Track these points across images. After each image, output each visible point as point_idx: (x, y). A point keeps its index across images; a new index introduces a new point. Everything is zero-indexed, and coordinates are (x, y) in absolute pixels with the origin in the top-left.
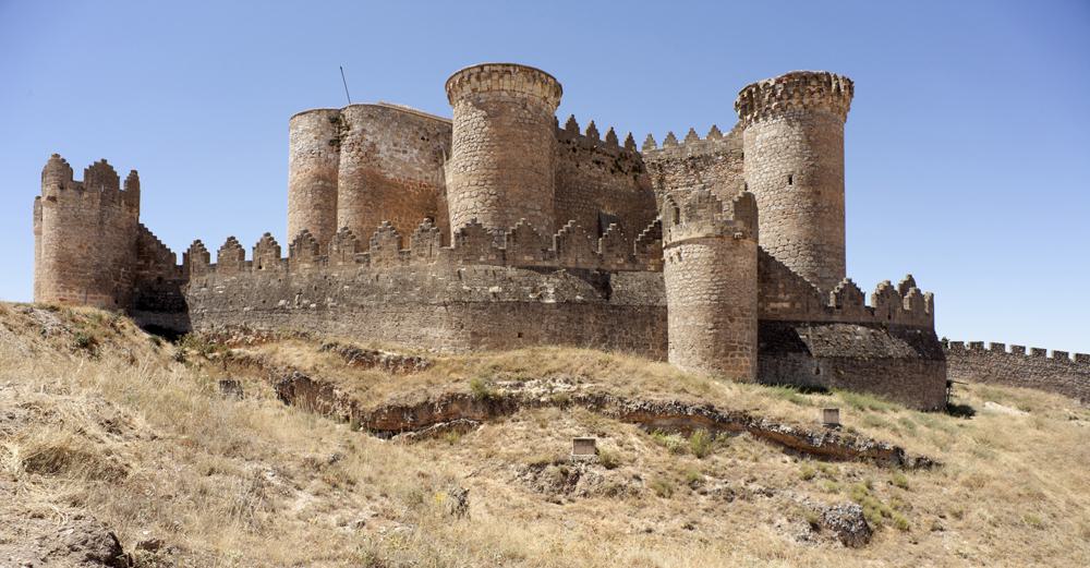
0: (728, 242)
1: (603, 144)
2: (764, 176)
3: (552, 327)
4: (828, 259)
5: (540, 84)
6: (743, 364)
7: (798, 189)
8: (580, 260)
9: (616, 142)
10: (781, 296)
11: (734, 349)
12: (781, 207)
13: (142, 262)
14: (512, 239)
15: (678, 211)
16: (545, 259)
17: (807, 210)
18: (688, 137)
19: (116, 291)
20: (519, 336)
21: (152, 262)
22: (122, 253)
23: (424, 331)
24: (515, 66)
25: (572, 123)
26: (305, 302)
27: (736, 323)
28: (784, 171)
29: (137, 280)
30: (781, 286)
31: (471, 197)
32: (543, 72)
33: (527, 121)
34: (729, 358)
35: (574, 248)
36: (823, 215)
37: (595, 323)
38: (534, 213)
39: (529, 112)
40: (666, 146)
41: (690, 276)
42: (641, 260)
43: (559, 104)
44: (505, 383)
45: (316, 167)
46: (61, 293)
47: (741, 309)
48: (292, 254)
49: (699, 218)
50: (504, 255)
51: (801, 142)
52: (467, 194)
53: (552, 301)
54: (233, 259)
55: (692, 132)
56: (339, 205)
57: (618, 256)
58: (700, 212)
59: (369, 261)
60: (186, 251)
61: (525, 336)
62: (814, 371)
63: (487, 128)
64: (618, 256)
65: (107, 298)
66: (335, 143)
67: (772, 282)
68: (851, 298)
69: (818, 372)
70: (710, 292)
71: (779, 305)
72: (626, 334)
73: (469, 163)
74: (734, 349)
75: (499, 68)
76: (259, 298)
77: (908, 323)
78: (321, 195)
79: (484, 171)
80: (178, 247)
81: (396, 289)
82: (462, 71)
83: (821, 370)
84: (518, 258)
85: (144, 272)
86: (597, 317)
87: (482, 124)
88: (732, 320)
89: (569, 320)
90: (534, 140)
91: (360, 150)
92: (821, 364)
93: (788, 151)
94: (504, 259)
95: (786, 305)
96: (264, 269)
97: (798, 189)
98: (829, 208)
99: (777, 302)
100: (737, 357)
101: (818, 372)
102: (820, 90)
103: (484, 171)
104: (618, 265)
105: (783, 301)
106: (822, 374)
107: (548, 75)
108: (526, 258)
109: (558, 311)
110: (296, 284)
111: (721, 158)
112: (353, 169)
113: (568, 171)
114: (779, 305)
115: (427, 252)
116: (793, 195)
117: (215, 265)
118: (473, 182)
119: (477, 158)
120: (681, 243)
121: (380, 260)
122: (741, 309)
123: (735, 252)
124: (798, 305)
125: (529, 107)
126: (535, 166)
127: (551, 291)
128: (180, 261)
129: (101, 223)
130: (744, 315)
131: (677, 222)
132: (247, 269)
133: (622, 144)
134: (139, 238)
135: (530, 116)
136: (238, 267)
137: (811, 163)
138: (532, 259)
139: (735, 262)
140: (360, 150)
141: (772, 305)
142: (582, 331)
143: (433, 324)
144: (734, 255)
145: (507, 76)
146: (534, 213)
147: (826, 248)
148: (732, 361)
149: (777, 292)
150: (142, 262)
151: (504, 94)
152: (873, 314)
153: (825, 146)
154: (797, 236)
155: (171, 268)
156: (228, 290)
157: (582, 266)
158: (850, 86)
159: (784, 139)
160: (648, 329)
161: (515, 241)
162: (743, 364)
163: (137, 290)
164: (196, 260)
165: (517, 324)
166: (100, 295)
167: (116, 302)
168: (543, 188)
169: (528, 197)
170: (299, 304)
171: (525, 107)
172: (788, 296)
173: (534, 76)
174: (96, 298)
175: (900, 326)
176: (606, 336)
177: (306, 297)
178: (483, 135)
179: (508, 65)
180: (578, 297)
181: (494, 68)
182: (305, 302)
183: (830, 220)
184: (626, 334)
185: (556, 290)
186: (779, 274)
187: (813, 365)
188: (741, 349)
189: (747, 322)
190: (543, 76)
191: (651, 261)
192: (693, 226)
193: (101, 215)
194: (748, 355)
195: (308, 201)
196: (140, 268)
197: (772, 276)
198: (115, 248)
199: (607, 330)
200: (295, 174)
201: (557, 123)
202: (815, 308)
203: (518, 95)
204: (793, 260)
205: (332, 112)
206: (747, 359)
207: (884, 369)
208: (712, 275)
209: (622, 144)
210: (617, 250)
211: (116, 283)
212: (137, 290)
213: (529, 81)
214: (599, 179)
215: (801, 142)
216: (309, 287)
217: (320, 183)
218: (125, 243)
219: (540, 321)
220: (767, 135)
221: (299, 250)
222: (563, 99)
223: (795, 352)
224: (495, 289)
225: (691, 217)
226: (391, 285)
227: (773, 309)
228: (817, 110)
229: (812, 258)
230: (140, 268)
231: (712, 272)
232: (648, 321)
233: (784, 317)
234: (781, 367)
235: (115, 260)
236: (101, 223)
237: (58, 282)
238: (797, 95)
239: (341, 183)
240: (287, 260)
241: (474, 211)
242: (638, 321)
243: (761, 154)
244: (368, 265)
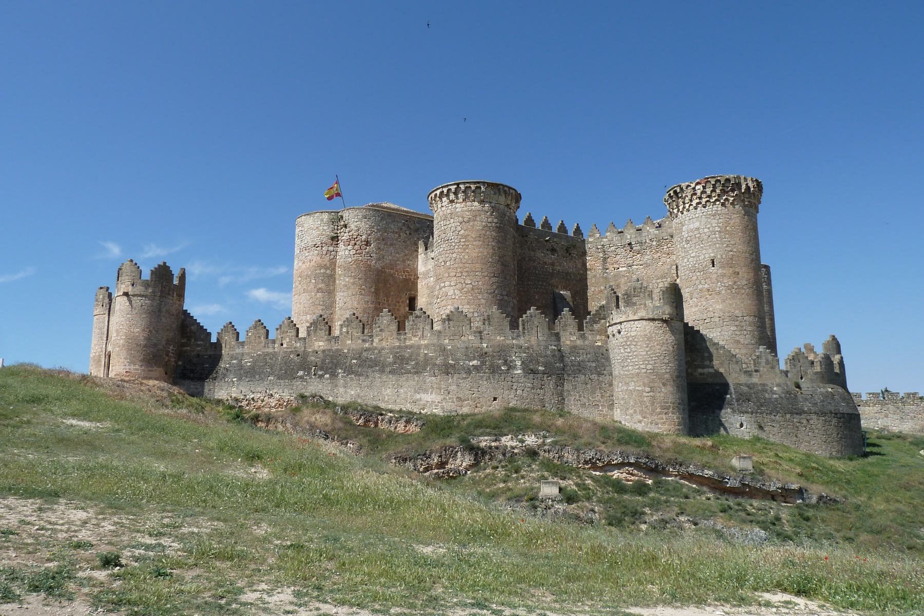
1: (555, 235)
2: (691, 259)
5: (503, 195)
7: (720, 271)
9: (566, 232)
12: (706, 286)
13: (184, 341)
14: (487, 323)
15: (617, 298)
16: (513, 339)
17: (730, 288)
19: (166, 365)
21: (193, 340)
22: (172, 334)
23: (418, 396)
25: (530, 220)
26: (320, 373)
28: (707, 256)
29: (180, 355)
31: (450, 286)
32: (506, 186)
41: (629, 350)
42: (590, 337)
43: (519, 207)
44: (486, 438)
45: (319, 258)
46: (128, 367)
48: (309, 334)
49: (635, 304)
51: (720, 232)
52: (447, 283)
53: (519, 372)
54: (259, 337)
56: (338, 288)
58: (635, 299)
59: (372, 341)
60: (220, 331)
63: (462, 231)
65: (159, 371)
70: (646, 362)
71: (706, 370)
73: (448, 259)
76: (281, 370)
78: (323, 280)
79: (461, 265)
80: (214, 329)
81: (395, 363)
82: (442, 187)
85: (186, 348)
87: (459, 228)
91: (355, 244)
93: (710, 239)
94: (481, 338)
96: (285, 346)
97: (720, 271)
99: (703, 368)
103: (461, 265)
104: (571, 341)
110: (313, 358)
111: (654, 243)
112: (350, 260)
113: (527, 259)
115: (420, 333)
117: (244, 342)
118: (453, 274)
119: (454, 255)
120: (621, 323)
121: (382, 340)
127: (519, 363)
128: (214, 339)
129: (160, 311)
131: (618, 306)
132: (270, 345)
133: (571, 233)
134: (183, 321)
136: (263, 344)
137: (729, 249)
140: (355, 244)
141: (700, 370)
143: (425, 391)
150: (184, 341)
154: (721, 310)
155: (208, 345)
156: (255, 362)
158: (759, 185)
159: (706, 230)
160: (598, 393)
161: (489, 324)
163: (180, 363)
164: (228, 338)
166: (155, 368)
167: (166, 374)
168: (508, 277)
170: (315, 375)
173: (499, 190)
174: (152, 371)
177: (321, 369)
178: (459, 237)
180: (540, 368)
182: (320, 373)
185: (523, 363)
190: (506, 189)
191: (598, 337)
192: (629, 311)
193: (160, 305)
195: (312, 286)
196: (183, 345)
198: (168, 330)
200: (300, 264)
201: (517, 220)
202: (736, 372)
204: (719, 330)
208: (647, 349)
209: (571, 233)
211: (167, 358)
212: (180, 363)
213: (495, 194)
214: (553, 264)
215: (720, 232)
216: (323, 361)
217: (322, 271)
218: (174, 326)
220: (691, 226)
221: (315, 331)
222: (522, 203)
224: (475, 362)
225: (629, 303)
226: (391, 360)
230: (183, 345)
231: (647, 347)
233: (710, 380)
235: (168, 340)
236: (160, 311)
237: (125, 359)
239: (339, 271)
240: (305, 339)
241: (453, 297)
243: (687, 242)
244: (372, 344)
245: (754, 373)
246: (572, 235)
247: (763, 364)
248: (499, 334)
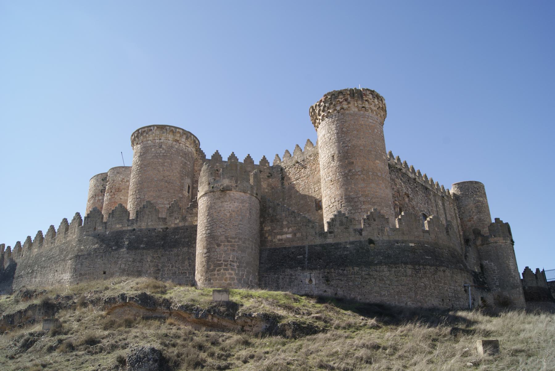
0: (218, 194)
3: (123, 266)
4: (364, 207)
6: (228, 276)
8: (149, 224)
10: (285, 230)
11: (220, 265)
12: (330, 178)
16: (128, 226)
18: (295, 150)
20: (105, 273)
24: (154, 126)
27: (222, 247)
28: (329, 154)
30: (285, 223)
33: (161, 154)
34: (216, 272)
35: (146, 217)
36: (357, 177)
37: (151, 261)
38: (163, 206)
39: (163, 149)
40: (285, 159)
47: (227, 237)
50: (106, 226)
55: (298, 146)
57: (175, 218)
61: (107, 273)
62: (307, 281)
64: (175, 218)
66: (103, 191)
67: (278, 221)
68: (342, 224)
69: (311, 281)
71: (284, 237)
72: (172, 267)
74: (220, 265)
75: (146, 129)
77: (399, 238)
83: (313, 280)
84: (113, 226)
86: (153, 257)
87: (138, 161)
88: (219, 245)
89: (134, 261)
90: (166, 164)
92: (312, 275)
93: (331, 141)
94: (106, 228)
95: (289, 236)
98: (362, 171)
100: (222, 271)
101: (311, 281)
102: (346, 100)
104: (175, 224)
105: (286, 233)
106: (314, 282)
107: (176, 128)
108: (118, 226)
109: (128, 255)
114: (284, 237)
116: (335, 168)
122: (227, 237)
123: (222, 200)
124: (298, 235)
125: (164, 146)
126: (166, 179)
130: (228, 241)
135: (163, 151)
138: (121, 226)
139: (223, 207)
141: (279, 237)
142: (142, 267)
144: (222, 202)
145: (150, 133)
146: (163, 206)
147: (362, 199)
148: (218, 275)
149: (282, 227)
151: (150, 142)
152: (361, 234)
153: (355, 132)
157: (151, 227)
159: (328, 135)
160: (186, 263)
161: (113, 217)
162: (228, 276)
165: (103, 266)
168: (172, 191)
169: (159, 197)
171: (161, 147)
172: (290, 230)
175: (389, 242)
176: (159, 270)
179: (150, 126)
181: (144, 130)
183: (364, 180)
184: (172, 267)
186: (284, 215)
187: (306, 277)
188: (226, 265)
189: (231, 246)
194: (232, 269)
197: (278, 217)
199: (160, 265)
203: (157, 141)
205: (104, 175)
206: (233, 272)
207: (369, 274)
210: (175, 215)
219: (116, 263)
223: (291, 268)
227: (279, 240)
228: (347, 112)
229: (351, 208)
232: (187, 257)
233: (288, 245)
234: (280, 281)
238: (332, 106)
242: (180, 258)
245: (329, 235)
246: (258, 164)
247: (338, 225)
248: (118, 223)
